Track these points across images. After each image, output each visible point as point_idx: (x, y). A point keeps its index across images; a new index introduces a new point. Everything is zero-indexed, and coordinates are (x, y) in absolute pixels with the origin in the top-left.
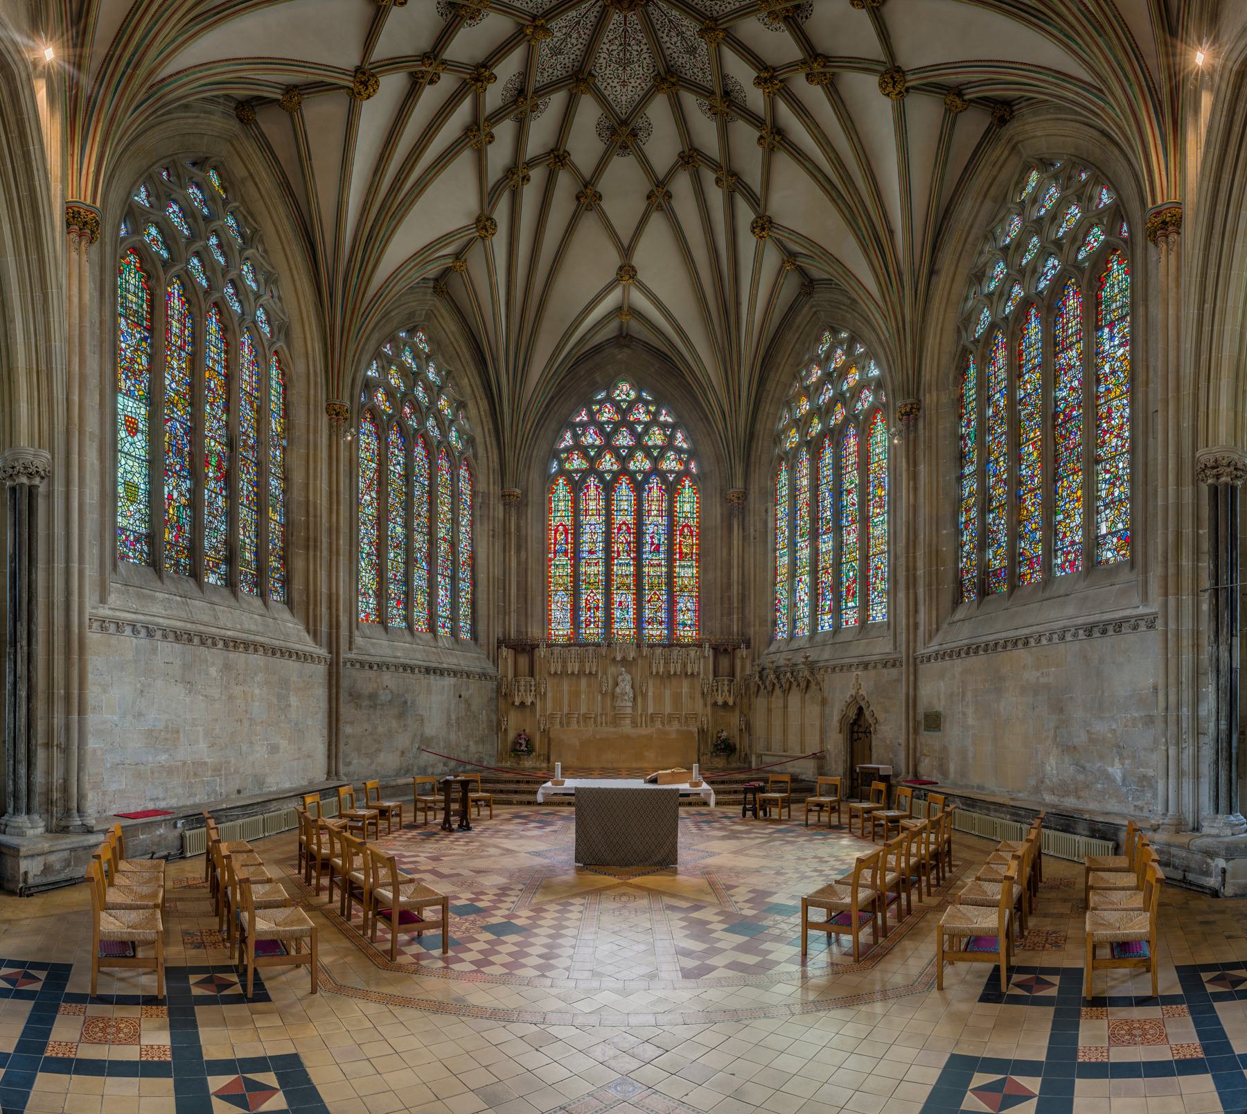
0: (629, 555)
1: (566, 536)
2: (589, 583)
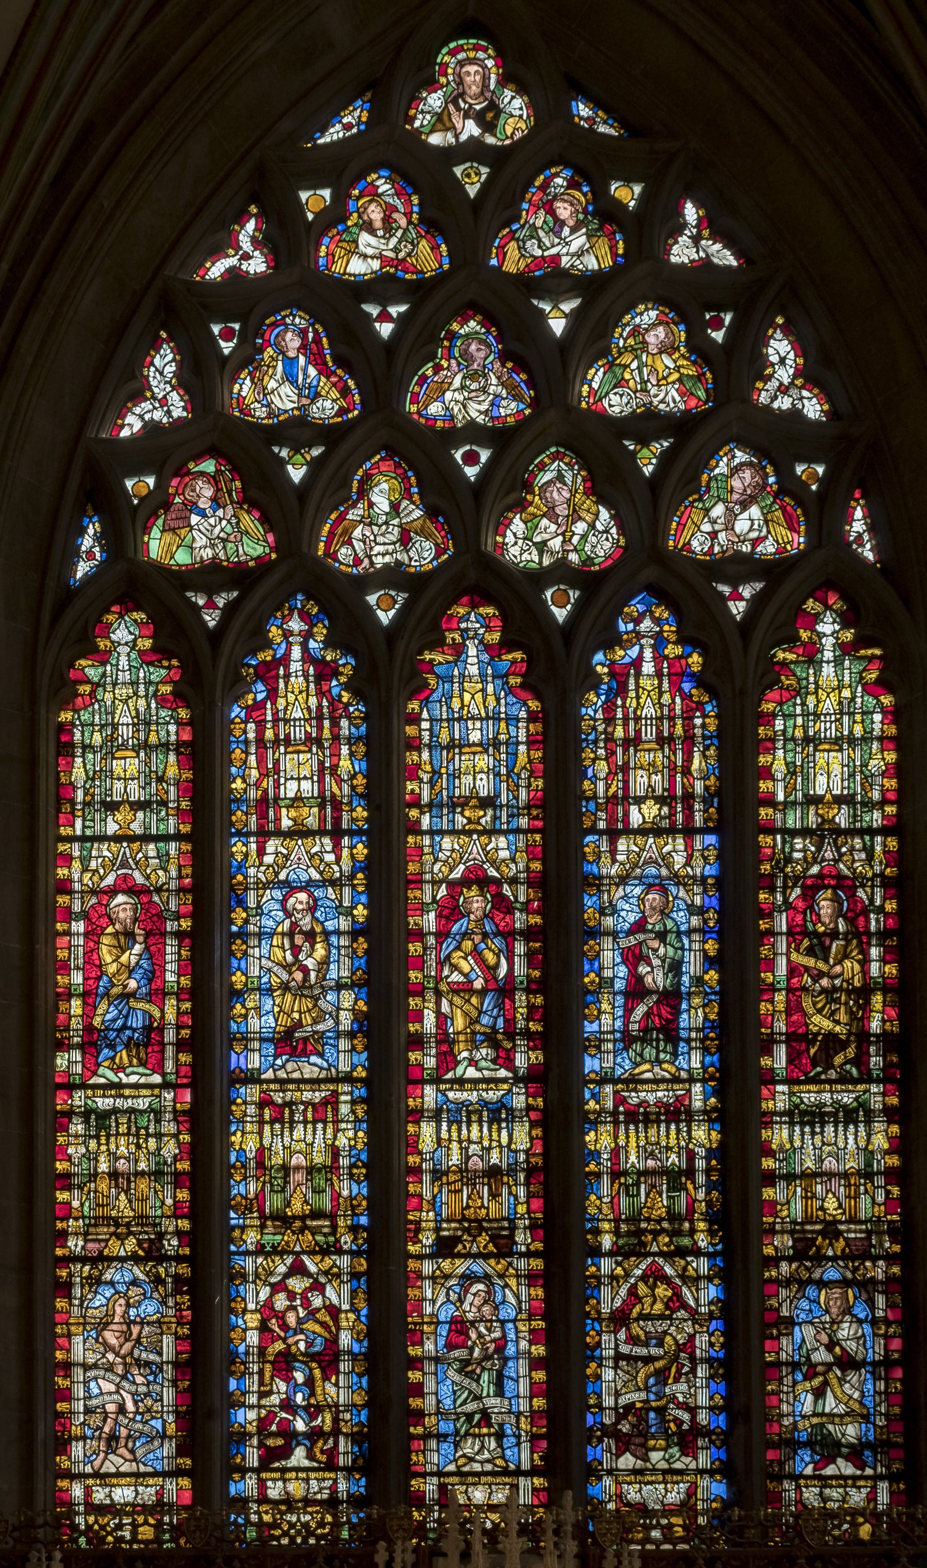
0: (504, 1059)
1: (154, 955)
2: (283, 1220)
